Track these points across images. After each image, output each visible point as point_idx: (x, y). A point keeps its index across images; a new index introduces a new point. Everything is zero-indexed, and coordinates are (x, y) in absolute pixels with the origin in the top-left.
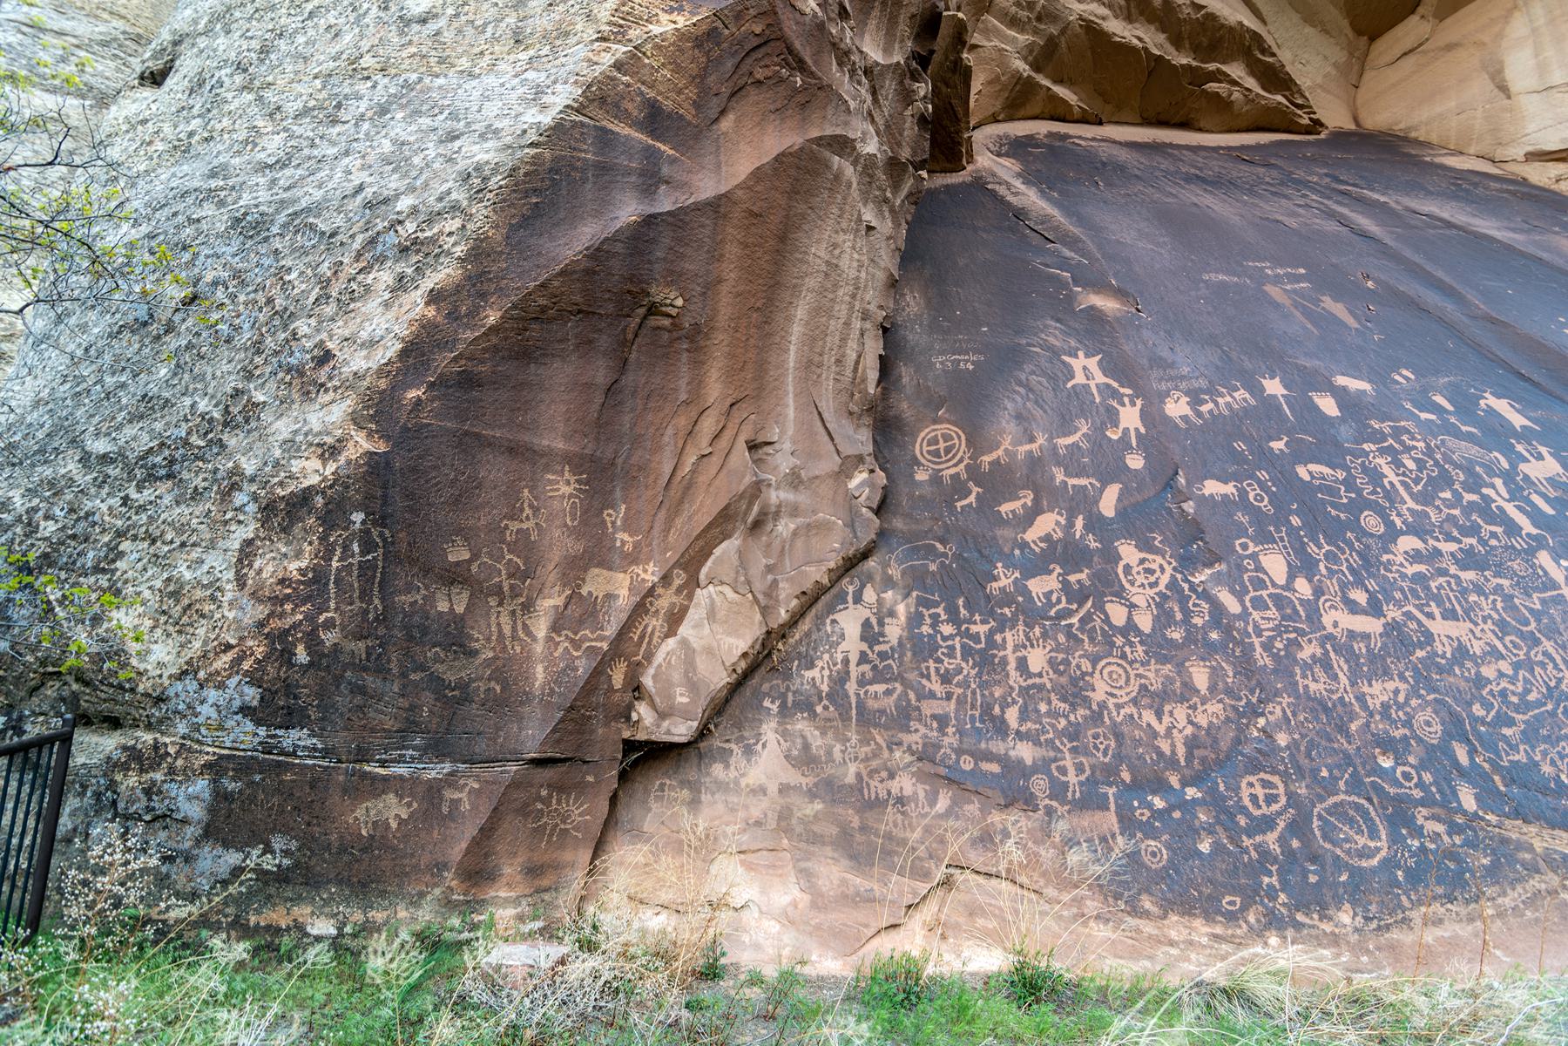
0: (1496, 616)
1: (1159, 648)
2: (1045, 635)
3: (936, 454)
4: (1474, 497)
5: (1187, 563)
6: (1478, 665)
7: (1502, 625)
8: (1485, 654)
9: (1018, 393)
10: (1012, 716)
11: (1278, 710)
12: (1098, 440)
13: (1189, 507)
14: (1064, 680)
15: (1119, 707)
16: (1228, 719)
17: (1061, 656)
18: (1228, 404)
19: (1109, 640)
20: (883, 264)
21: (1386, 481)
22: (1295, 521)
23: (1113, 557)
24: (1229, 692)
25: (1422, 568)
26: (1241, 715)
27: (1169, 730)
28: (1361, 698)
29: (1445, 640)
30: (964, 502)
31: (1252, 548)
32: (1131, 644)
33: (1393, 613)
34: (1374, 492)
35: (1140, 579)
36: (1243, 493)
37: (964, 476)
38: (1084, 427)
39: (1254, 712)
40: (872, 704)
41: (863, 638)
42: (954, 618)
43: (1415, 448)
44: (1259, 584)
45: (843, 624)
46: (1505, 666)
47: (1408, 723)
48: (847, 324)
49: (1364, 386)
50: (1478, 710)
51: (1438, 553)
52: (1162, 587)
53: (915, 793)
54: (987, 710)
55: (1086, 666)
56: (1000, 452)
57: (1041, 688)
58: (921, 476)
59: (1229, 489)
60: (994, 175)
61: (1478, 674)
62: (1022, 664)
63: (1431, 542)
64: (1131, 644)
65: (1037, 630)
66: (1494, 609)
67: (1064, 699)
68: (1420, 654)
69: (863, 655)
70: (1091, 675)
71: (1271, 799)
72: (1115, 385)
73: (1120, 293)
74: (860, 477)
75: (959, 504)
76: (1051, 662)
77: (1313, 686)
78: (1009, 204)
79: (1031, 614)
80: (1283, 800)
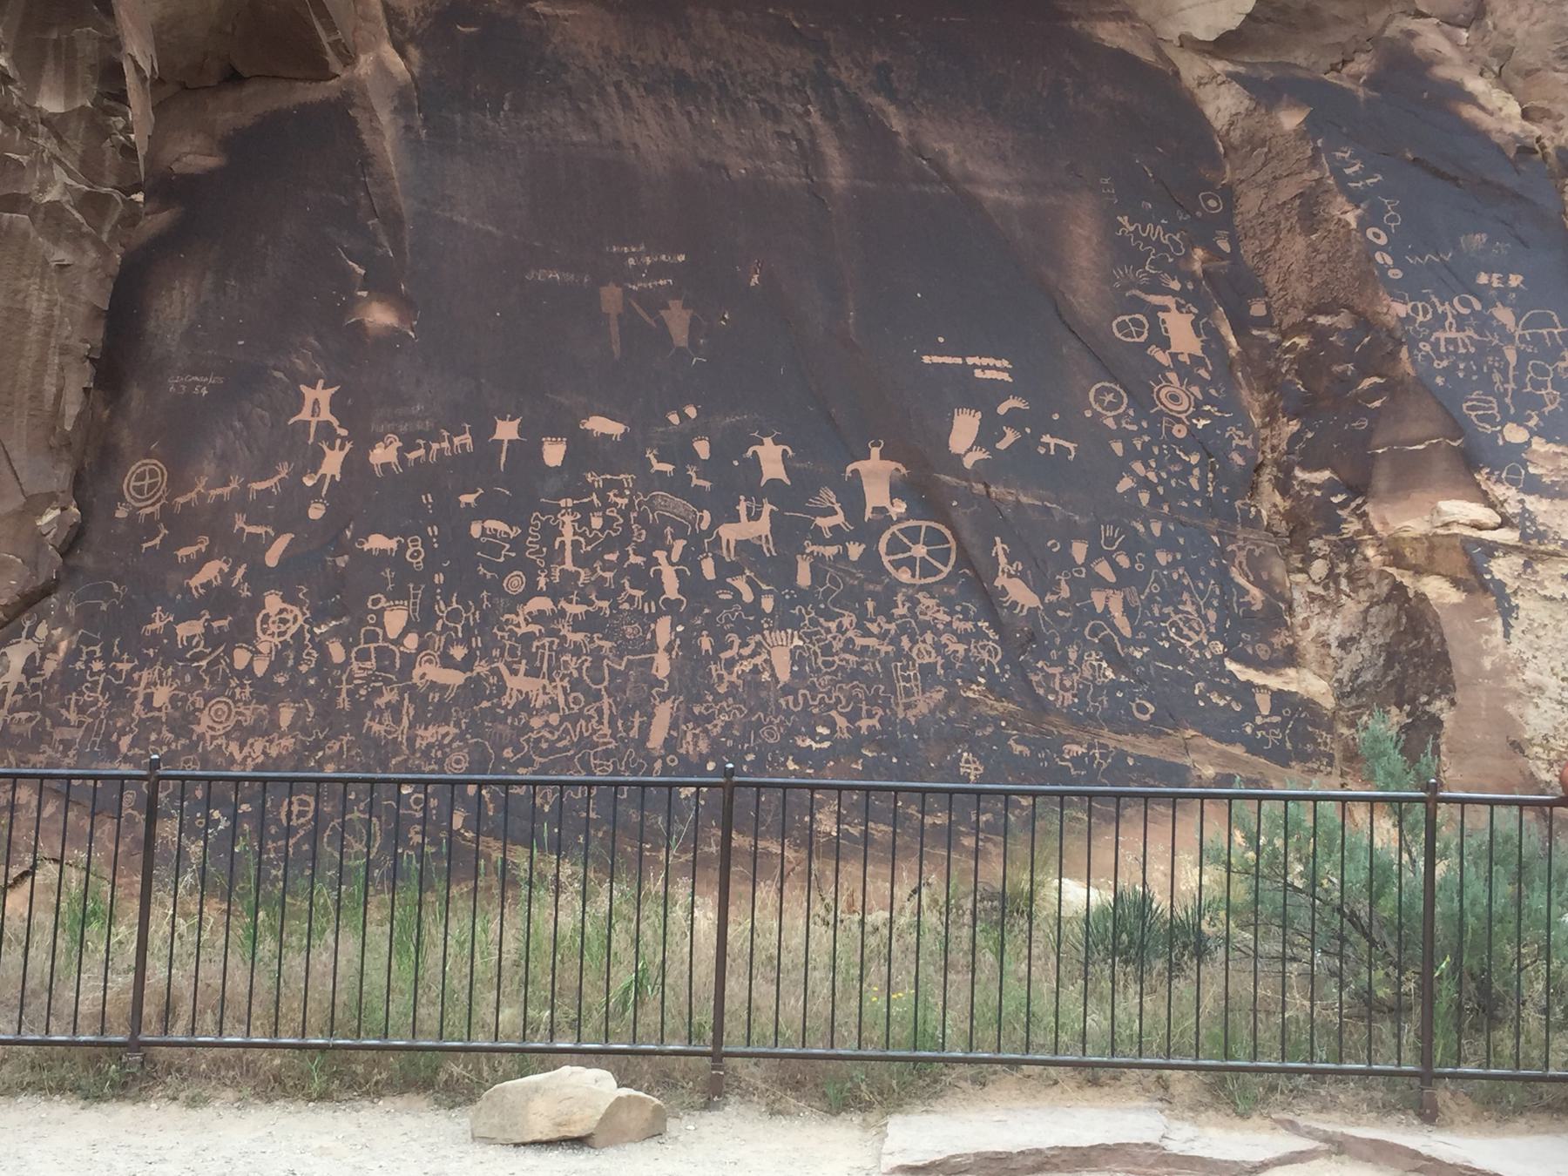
0: (576, 674)
1: (265, 691)
2: (174, 676)
3: (139, 490)
4: (639, 560)
5: (318, 617)
6: (531, 716)
7: (576, 684)
8: (544, 706)
9: (232, 427)
10: (125, 742)
11: (337, 747)
12: (293, 485)
13: (342, 562)
14: (177, 714)
15: (213, 738)
16: (295, 751)
17: (182, 694)
18: (441, 451)
19: (222, 681)
20: (83, 298)
21: (559, 539)
22: (439, 578)
23: (257, 604)
24: (306, 731)
25: (535, 628)
26: (306, 748)
27: (245, 759)
28: (411, 740)
29: (515, 693)
30: (150, 544)
31: (383, 603)
32: (242, 686)
33: (481, 668)
34: (539, 551)
35: (273, 628)
36: (402, 548)
37: (157, 517)
38: (284, 471)
39: (318, 745)
40: (14, 729)
41: (24, 671)
42: (107, 657)
43: (616, 504)
44: (372, 637)
45: (10, 657)
46: (554, 719)
47: (440, 762)
48: (42, 361)
49: (615, 429)
50: (508, 753)
51: (563, 613)
52: (287, 637)
53: (29, 802)
54: (108, 734)
55: (200, 703)
56: (193, 495)
57: (157, 720)
58: (121, 513)
59: (390, 544)
60: (364, 94)
61: (527, 724)
62: (149, 698)
63: (563, 604)
64: (242, 686)
65: (170, 670)
66: (579, 669)
67: (170, 731)
68: (485, 704)
69: (20, 685)
70: (201, 711)
71: (301, 814)
72: (336, 423)
73: (404, 305)
74: (51, 515)
75: (145, 545)
76: (173, 699)
77: (376, 727)
78: (361, 144)
79: (170, 653)
80: (310, 815)
